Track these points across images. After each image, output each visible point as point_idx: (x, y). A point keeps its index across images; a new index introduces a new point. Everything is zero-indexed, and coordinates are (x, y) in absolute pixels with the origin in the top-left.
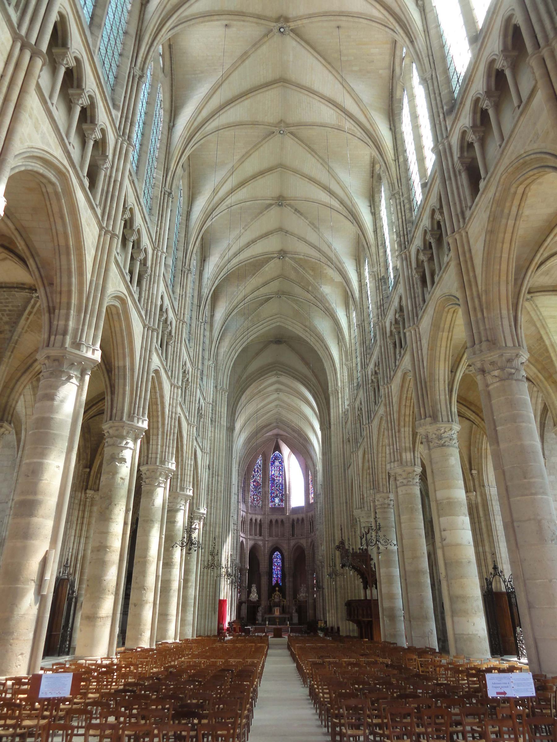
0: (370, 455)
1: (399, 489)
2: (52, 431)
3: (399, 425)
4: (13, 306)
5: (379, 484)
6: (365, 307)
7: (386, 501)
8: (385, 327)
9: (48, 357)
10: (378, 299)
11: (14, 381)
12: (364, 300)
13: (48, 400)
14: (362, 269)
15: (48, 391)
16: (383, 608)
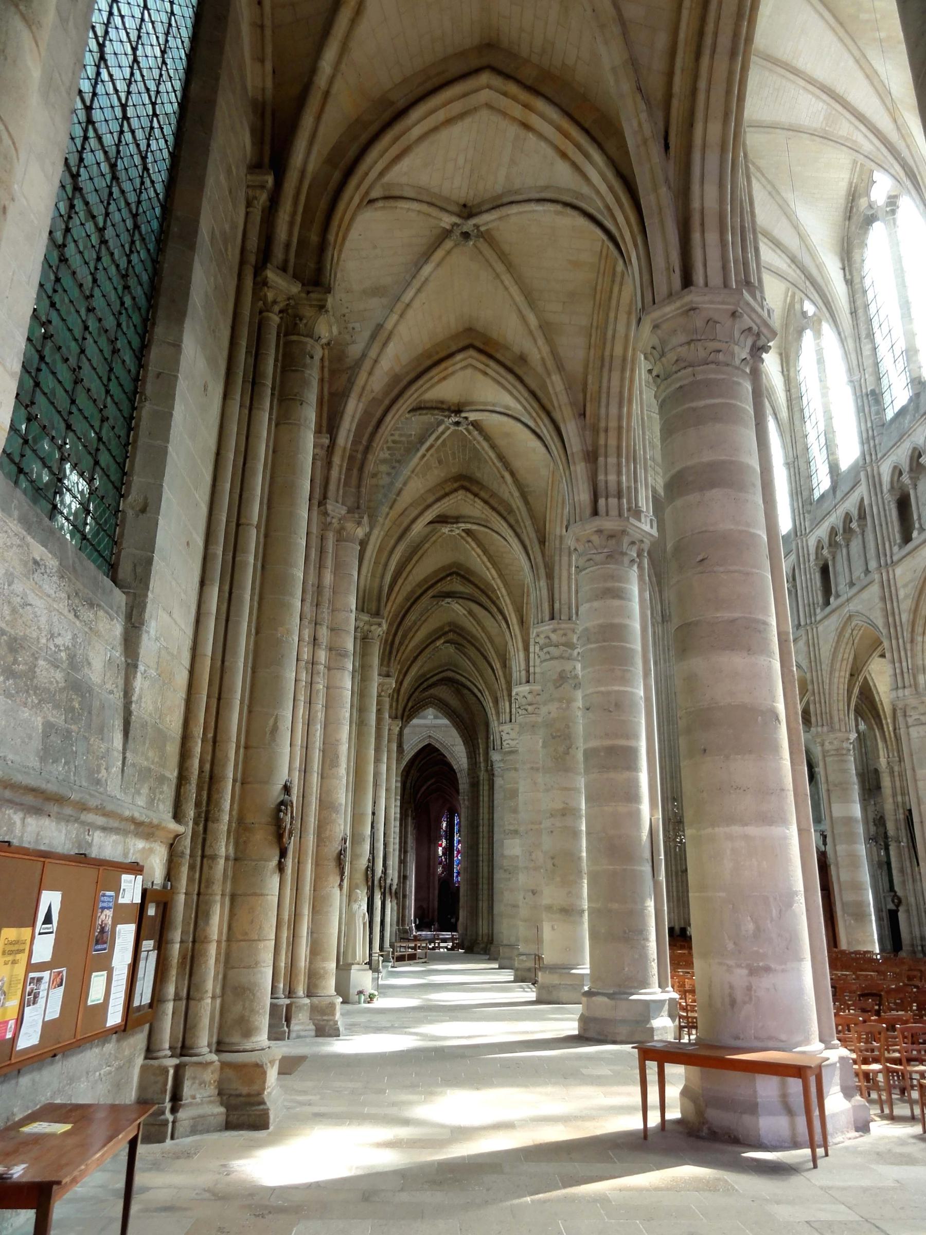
0: (814, 674)
1: (911, 729)
2: (628, 645)
3: (913, 631)
4: (401, 435)
5: (831, 718)
6: (799, 435)
7: (845, 745)
8: (879, 475)
9: (599, 532)
10: (863, 428)
11: (385, 554)
12: (797, 423)
13: (613, 598)
14: (792, 370)
15: (609, 584)
16: (843, 904)
